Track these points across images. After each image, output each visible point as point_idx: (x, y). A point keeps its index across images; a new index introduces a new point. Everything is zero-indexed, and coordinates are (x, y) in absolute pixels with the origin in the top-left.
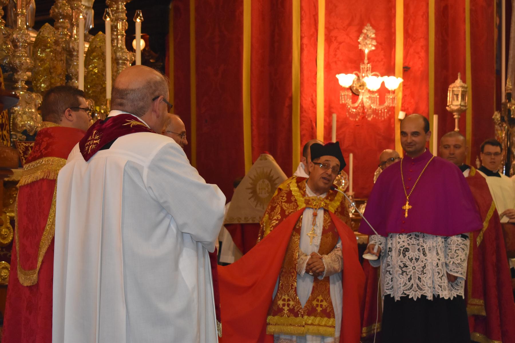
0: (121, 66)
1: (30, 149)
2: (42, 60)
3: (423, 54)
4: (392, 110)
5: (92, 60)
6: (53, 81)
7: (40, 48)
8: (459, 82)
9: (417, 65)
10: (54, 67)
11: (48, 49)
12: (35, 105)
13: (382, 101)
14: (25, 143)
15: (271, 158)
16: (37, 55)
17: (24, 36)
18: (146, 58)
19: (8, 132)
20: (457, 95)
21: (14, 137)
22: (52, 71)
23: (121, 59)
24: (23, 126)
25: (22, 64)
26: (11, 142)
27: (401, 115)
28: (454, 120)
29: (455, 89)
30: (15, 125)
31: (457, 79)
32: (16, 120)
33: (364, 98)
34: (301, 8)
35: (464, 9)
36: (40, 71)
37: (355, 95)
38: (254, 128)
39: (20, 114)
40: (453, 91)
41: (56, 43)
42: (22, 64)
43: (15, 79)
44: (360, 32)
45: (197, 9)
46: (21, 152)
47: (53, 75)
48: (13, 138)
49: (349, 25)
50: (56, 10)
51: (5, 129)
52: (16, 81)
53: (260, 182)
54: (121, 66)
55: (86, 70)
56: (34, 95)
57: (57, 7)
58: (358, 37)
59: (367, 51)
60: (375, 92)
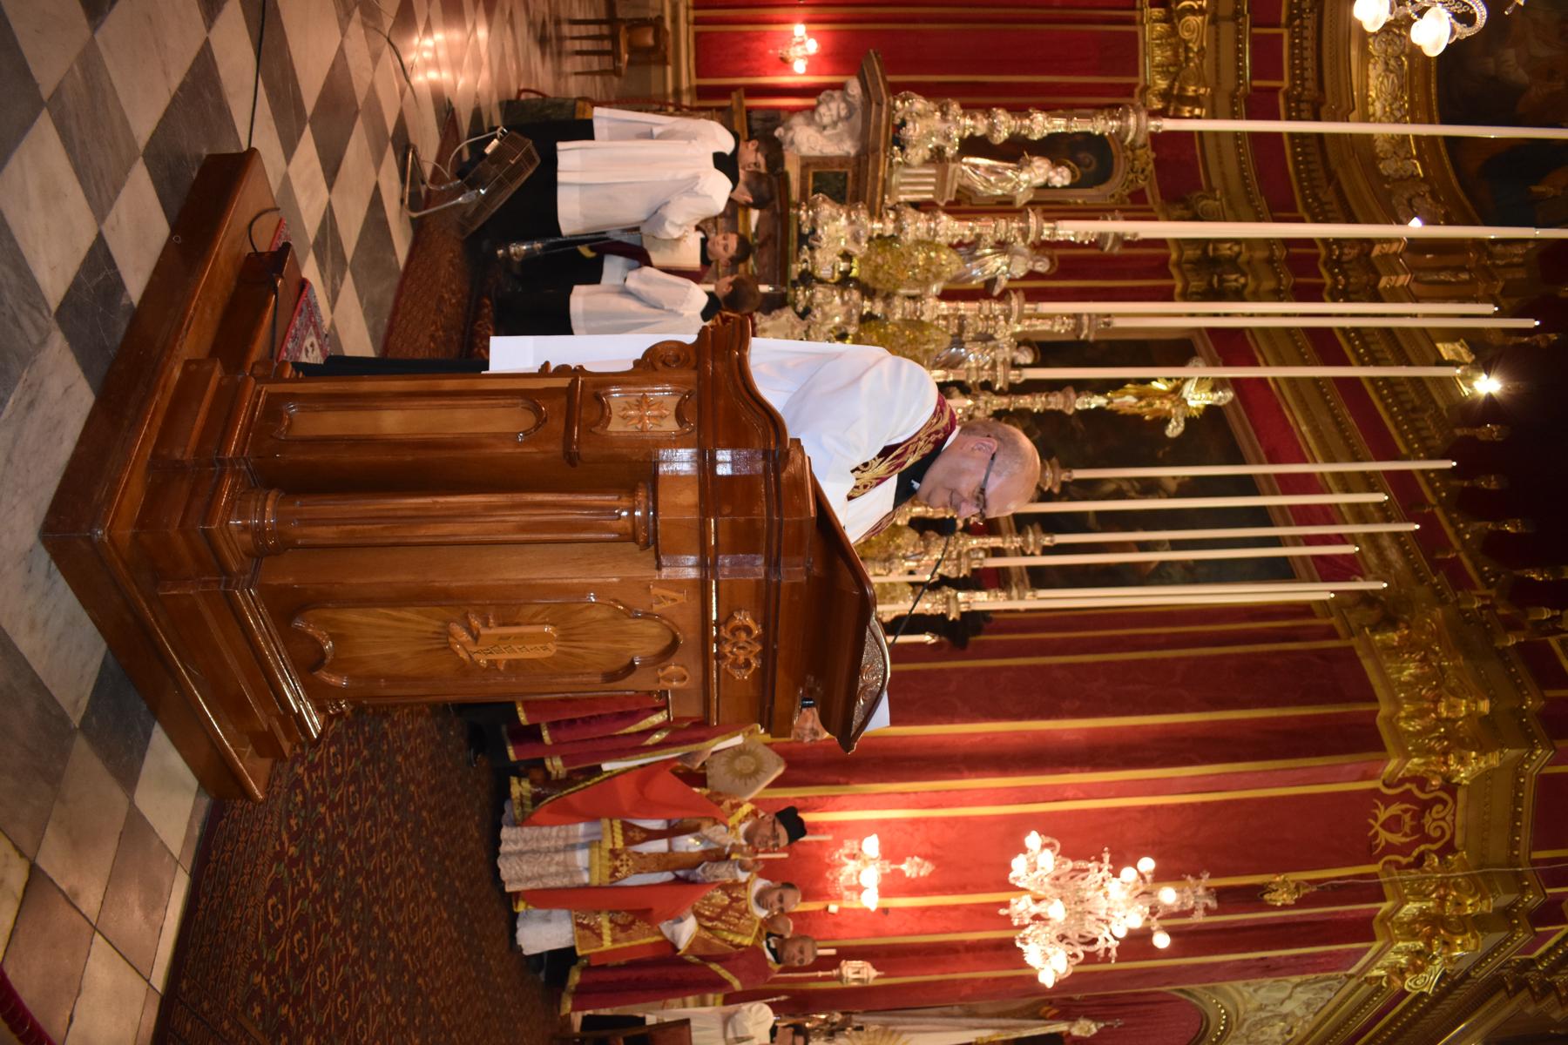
3: (904, 930)
4: (839, 898)
8: (874, 973)
9: (890, 923)
13: (849, 888)
15: (780, 771)
20: (858, 973)
27: (833, 908)
28: (830, 970)
29: (865, 970)
31: (878, 970)
33: (851, 866)
34: (948, 791)
35: (955, 972)
37: (853, 857)
40: (863, 968)
44: (926, 857)
45: (941, 671)
49: (933, 845)
53: (752, 760)
58: (919, 856)
59: (904, 867)
60: (858, 879)
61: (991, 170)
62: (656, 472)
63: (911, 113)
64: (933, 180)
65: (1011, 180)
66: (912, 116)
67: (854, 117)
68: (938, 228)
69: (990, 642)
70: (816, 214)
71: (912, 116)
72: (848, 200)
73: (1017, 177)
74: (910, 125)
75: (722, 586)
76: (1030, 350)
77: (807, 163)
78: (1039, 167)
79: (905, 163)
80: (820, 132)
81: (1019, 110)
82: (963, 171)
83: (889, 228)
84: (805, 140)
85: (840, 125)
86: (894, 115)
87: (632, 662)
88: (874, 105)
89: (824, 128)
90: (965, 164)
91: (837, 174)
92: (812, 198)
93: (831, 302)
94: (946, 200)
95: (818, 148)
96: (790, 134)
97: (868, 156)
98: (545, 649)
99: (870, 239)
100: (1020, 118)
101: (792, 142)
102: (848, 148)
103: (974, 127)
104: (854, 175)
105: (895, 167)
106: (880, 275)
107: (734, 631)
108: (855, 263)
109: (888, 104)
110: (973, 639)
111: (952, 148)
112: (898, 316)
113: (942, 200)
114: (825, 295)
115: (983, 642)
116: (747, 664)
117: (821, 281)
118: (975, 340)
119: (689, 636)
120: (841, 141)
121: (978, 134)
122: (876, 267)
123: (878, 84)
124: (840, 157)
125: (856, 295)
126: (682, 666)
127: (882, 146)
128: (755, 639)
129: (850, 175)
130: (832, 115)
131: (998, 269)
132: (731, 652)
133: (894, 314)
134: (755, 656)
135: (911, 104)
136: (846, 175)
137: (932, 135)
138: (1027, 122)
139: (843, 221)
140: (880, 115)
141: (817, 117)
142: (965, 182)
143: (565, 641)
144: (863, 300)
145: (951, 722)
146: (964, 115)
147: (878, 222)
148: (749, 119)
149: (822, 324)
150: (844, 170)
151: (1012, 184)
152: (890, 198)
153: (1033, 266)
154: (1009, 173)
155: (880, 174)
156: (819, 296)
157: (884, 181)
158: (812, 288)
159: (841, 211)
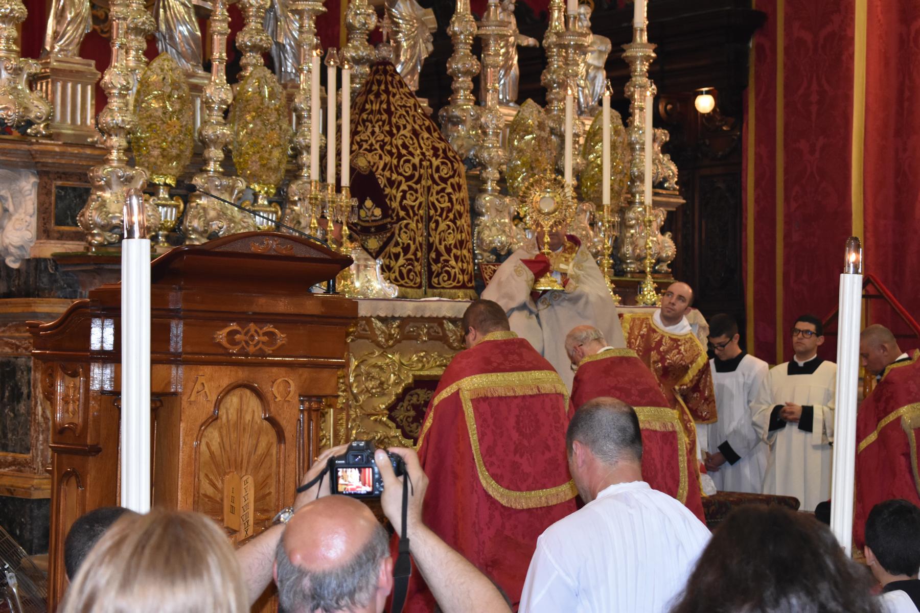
0: (638, 152)
2: (520, 151)
5: (594, 146)
7: (518, 134)
10: (537, 160)
11: (528, 135)
12: (509, 213)
14: (494, 266)
16: (513, 145)
17: (495, 119)
18: (717, 123)
19: (469, 251)
21: (480, 257)
22: (534, 165)
23: (638, 143)
24: (491, 242)
25: (492, 158)
26: (475, 264)
30: (481, 241)
32: (482, 235)
36: (518, 165)
38: (868, 235)
39: (488, 227)
41: (541, 126)
42: (492, 158)
43: (483, 178)
45: (787, 49)
47: (536, 171)
48: (478, 259)
50: (549, 77)
51: (465, 248)
52: (485, 182)
54: (638, 152)
55: (584, 162)
56: (507, 200)
61: (60, 16)
62: (110, 392)
64: (70, 85)
68: (119, 86)
70: (96, 225)
72: (87, 185)
75: (189, 349)
77: (44, 232)
79: (47, 119)
80: (11, 216)
82: (61, 50)
83: (116, 141)
84: (18, 233)
87: (266, 419)
90: (53, 47)
91: (59, 198)
92: (80, 228)
93: (204, 209)
94: (95, 71)
95: (28, 218)
96: (12, 250)
97: (39, 162)
99: (131, 163)
101: (21, 248)
102: (28, 185)
103: (8, 39)
104: (60, 178)
105: (52, 131)
106: (174, 152)
108: (158, 180)
110: (754, 7)
111: (30, 66)
112: (226, 131)
113: (95, 74)
114: (195, 217)
116: (270, 334)
117: (180, 220)
118: (274, 34)
119: (241, 374)
120: (20, 191)
121: (15, 34)
122: (164, 157)
124: (39, 195)
125: (198, 181)
126: (273, 383)
127: (26, 147)
128: (243, 328)
129: (59, 183)
132: (255, 346)
133: (224, 134)
134: (261, 329)
136: (57, 187)
137: (15, 88)
139: (107, 195)
143: (241, 468)
144: (207, 171)
147: (111, 153)
149: (231, 220)
150: (54, 190)
152: (92, 137)
155: (57, 149)
156: (195, 223)
157: (65, 144)
158: (187, 230)
159: (94, 197)
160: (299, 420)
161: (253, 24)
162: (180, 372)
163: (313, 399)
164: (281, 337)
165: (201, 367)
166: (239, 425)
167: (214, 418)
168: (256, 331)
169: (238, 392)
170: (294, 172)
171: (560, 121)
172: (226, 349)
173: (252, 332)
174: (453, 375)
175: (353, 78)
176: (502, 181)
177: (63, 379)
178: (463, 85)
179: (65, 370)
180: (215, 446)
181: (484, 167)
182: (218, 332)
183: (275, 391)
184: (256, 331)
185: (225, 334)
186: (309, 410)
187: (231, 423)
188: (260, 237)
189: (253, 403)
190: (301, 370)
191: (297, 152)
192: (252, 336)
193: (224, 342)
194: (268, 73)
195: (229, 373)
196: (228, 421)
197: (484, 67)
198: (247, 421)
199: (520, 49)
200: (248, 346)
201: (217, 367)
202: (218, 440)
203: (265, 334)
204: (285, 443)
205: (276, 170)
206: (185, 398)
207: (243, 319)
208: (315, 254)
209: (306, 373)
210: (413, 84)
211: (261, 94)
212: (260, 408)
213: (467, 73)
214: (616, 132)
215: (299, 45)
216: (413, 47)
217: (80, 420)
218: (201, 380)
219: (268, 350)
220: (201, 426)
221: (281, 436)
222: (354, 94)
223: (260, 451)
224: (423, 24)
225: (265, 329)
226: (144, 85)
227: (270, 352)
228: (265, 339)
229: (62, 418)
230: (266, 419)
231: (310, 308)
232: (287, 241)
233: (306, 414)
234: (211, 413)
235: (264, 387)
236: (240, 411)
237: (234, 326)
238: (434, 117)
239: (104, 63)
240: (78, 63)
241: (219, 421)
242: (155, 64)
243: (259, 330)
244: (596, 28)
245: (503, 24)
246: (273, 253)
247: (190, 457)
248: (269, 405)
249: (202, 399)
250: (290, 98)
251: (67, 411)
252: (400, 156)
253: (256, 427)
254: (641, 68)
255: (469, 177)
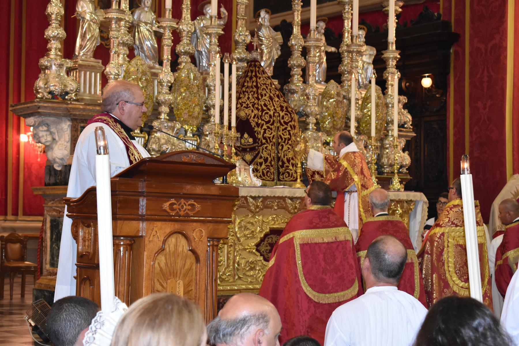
1: (316, 173)
2: (327, 108)
5: (367, 105)
6: (335, 123)
7: (326, 98)
10: (336, 113)
11: (332, 99)
12: (321, 141)
16: (323, 105)
18: (434, 93)
21: (305, 164)
22: (334, 115)
23: (390, 103)
25: (312, 112)
26: (303, 168)
36: (326, 115)
38: (515, 153)
41: (338, 94)
43: (307, 122)
46: (309, 175)
47: (335, 119)
50: (343, 68)
52: (308, 124)
54: (390, 108)
56: (320, 134)
57: (343, 66)
61: (83, 37)
63: (45, 88)
64: (88, 73)
65: (89, 25)
66: (47, 88)
67: (48, 122)
68: (114, 73)
69: (456, 15)
71: (47, 88)
73: (88, 20)
74: (52, 88)
75: (149, 213)
76: (206, 6)
78: (82, 7)
79: (76, 91)
80: (57, 142)
81: (46, 22)
82: (84, 55)
85: (53, 130)
86: (46, 99)
87: (190, 250)
88: (39, 110)
89: (54, 139)
90: (79, 53)
93: (159, 139)
95: (66, 144)
96: (57, 160)
97: (72, 114)
98: (179, 284)
100: (51, 21)
101: (62, 159)
103: (56, 49)
107: (173, 209)
109: (39, 102)
110: (453, 31)
111: (68, 63)
112: (170, 97)
113: (101, 67)
114: (153, 143)
115: (455, 19)
116: (192, 205)
118: (196, 46)
119: (177, 226)
120: (62, 129)
121: (59, 46)
123: (28, 107)
124: (72, 131)
125: (155, 124)
127: (65, 106)
128: (178, 202)
130: (46, 135)
131: (148, 30)
133: (169, 99)
134: (187, 202)
135: (40, 88)
137: (59, 75)
138: (53, 16)
140: (45, 107)
141: (48, 144)
142: (90, 54)
143: (176, 276)
144: (160, 119)
145: (506, 48)
146: (48, 55)
148: (49, 185)
149: (173, 144)
151: (92, 23)
152: (99, 100)
153: (148, 7)
154: (86, 26)
155: (81, 107)
157: (86, 104)
160: (207, 251)
161: (185, 40)
162: (144, 225)
163: (215, 240)
164: (198, 207)
165: (156, 222)
166: (175, 254)
167: (162, 250)
168: (185, 203)
169: (175, 236)
170: (206, 120)
171: (349, 91)
172: (168, 213)
173: (183, 204)
174: (291, 227)
175: (238, 69)
176: (317, 124)
177: (83, 229)
178: (297, 72)
179: (83, 224)
180: (163, 265)
181: (307, 116)
182: (164, 204)
183: (195, 235)
184: (185, 203)
185: (168, 205)
186: (213, 246)
187: (171, 252)
188: (187, 154)
189: (183, 242)
190: (208, 224)
191: (208, 109)
192: (183, 206)
193: (168, 209)
194: (193, 66)
195: (170, 225)
196: (170, 251)
197: (308, 63)
198: (180, 251)
199: (327, 53)
200: (180, 211)
201: (164, 223)
202: (164, 261)
203: (189, 205)
204: (200, 263)
205: (197, 118)
206: (147, 239)
207: (178, 197)
208: (216, 162)
209: (211, 226)
210: (270, 72)
211: (189, 77)
212: (187, 245)
213: (299, 66)
214: (379, 97)
215: (209, 51)
216: (270, 52)
217: (92, 250)
218: (155, 229)
219: (191, 213)
220: (155, 254)
221: (198, 260)
222: (238, 77)
223: (187, 267)
224: (275, 40)
225: (189, 202)
226: (127, 73)
227: (192, 215)
228: (189, 207)
229: (82, 249)
230: (190, 250)
231: (213, 191)
232: (201, 155)
233: (211, 248)
234: (160, 247)
235: (189, 233)
236: (176, 246)
237: (173, 201)
238: (281, 90)
239: (106, 61)
240: (93, 61)
241: (165, 251)
242: (133, 62)
243: (186, 203)
244: (368, 42)
245: (318, 40)
246: (194, 162)
247: (149, 270)
248: (191, 243)
249: (156, 239)
250: (205, 80)
251: (85, 246)
252: (263, 110)
253: (184, 254)
254: (392, 63)
255: (299, 122)
